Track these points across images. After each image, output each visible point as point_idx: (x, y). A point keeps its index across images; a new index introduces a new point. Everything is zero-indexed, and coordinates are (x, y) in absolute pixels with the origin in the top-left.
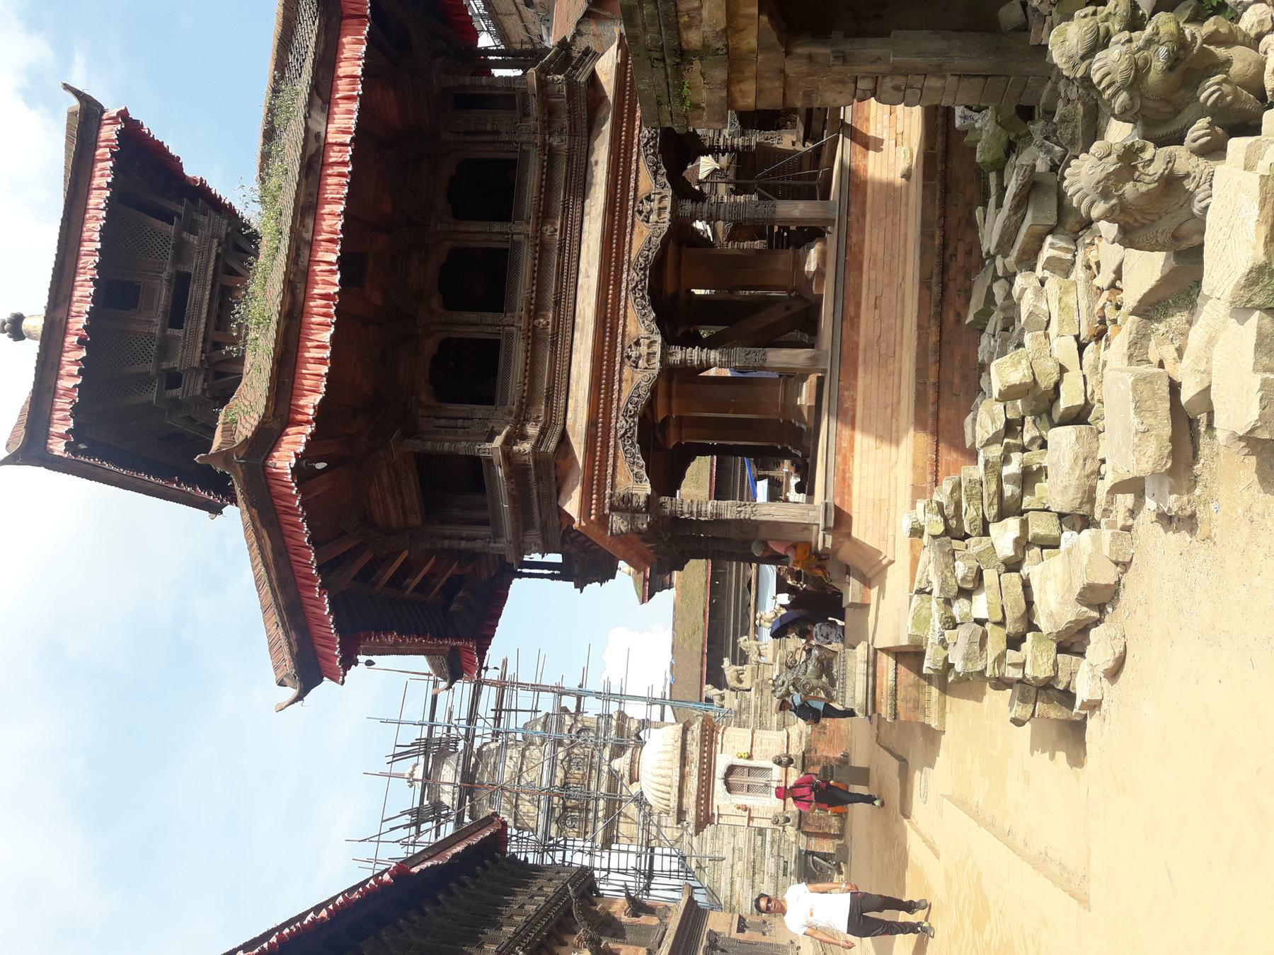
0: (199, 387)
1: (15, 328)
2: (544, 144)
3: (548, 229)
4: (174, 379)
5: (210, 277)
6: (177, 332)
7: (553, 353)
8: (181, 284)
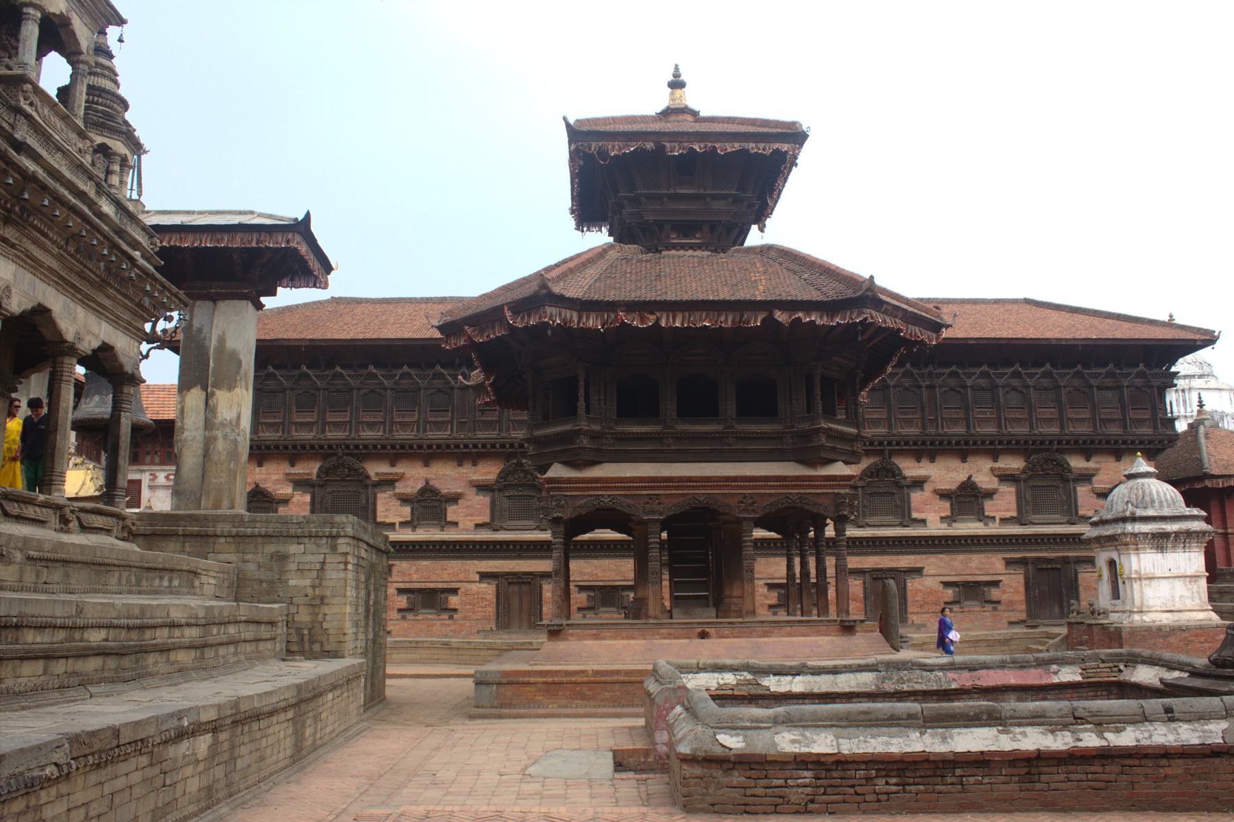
1: (677, 84)
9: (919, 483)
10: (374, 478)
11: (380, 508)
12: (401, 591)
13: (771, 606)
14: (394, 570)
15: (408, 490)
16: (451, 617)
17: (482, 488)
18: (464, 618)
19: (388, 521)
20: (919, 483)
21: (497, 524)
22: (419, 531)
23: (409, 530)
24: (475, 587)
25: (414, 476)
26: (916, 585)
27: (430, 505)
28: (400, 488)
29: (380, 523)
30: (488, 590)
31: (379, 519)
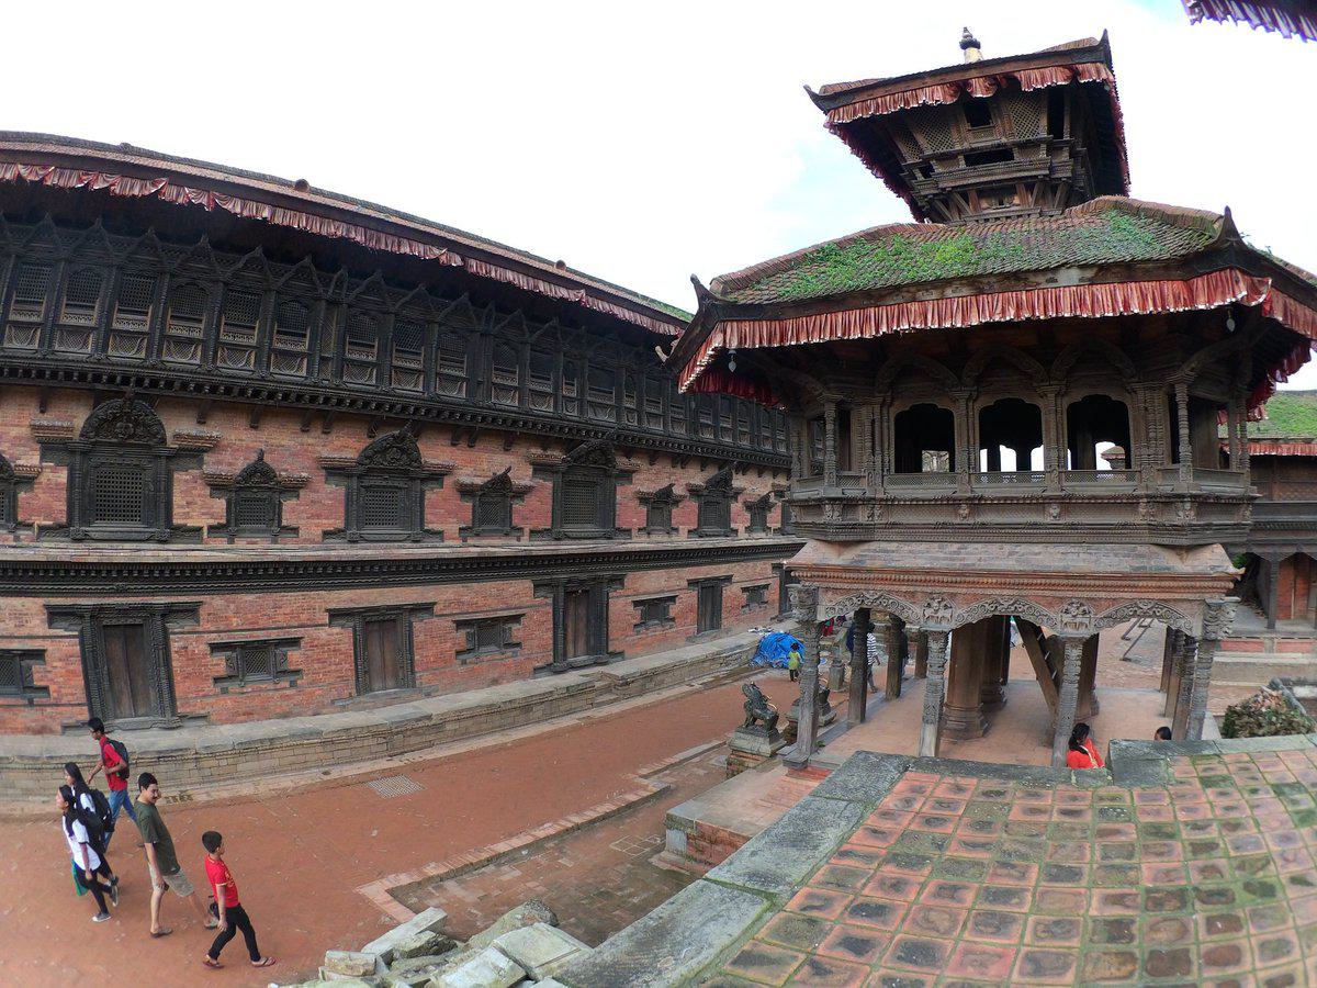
0: (927, 192)
2: (1138, 497)
3: (1054, 510)
4: (927, 171)
5: (1015, 175)
6: (962, 164)
7: (937, 526)
8: (1002, 154)
10: (172, 444)
11: (178, 499)
14: (203, 611)
15: (224, 470)
16: (293, 684)
17: (334, 470)
18: (312, 683)
19: (191, 523)
22: (240, 543)
23: (222, 543)
24: (323, 634)
25: (238, 445)
27: (255, 498)
28: (212, 465)
29: (179, 528)
30: (341, 637)
31: (177, 521)
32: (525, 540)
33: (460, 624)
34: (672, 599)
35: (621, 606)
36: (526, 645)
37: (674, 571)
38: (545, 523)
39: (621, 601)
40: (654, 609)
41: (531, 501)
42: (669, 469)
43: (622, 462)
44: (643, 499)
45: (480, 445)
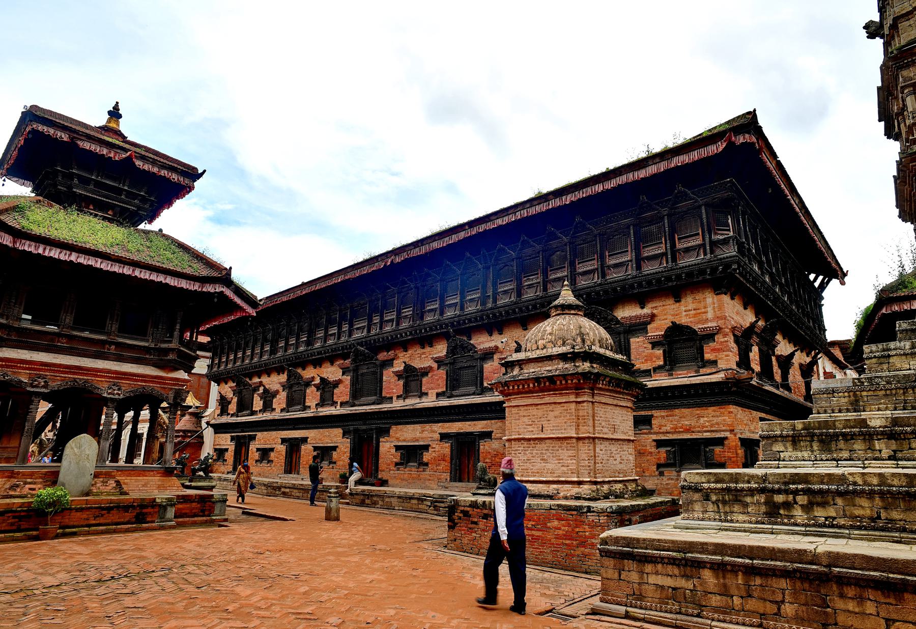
1: (115, 114)
9: (488, 355)
12: (258, 450)
13: (397, 464)
20: (488, 355)
21: (290, 409)
26: (486, 447)
32: (338, 407)
33: (316, 448)
34: (426, 448)
35: (387, 448)
36: (338, 463)
37: (427, 426)
38: (346, 398)
39: (388, 445)
40: (411, 454)
41: (341, 387)
42: (420, 351)
43: (383, 356)
44: (399, 375)
45: (324, 365)
